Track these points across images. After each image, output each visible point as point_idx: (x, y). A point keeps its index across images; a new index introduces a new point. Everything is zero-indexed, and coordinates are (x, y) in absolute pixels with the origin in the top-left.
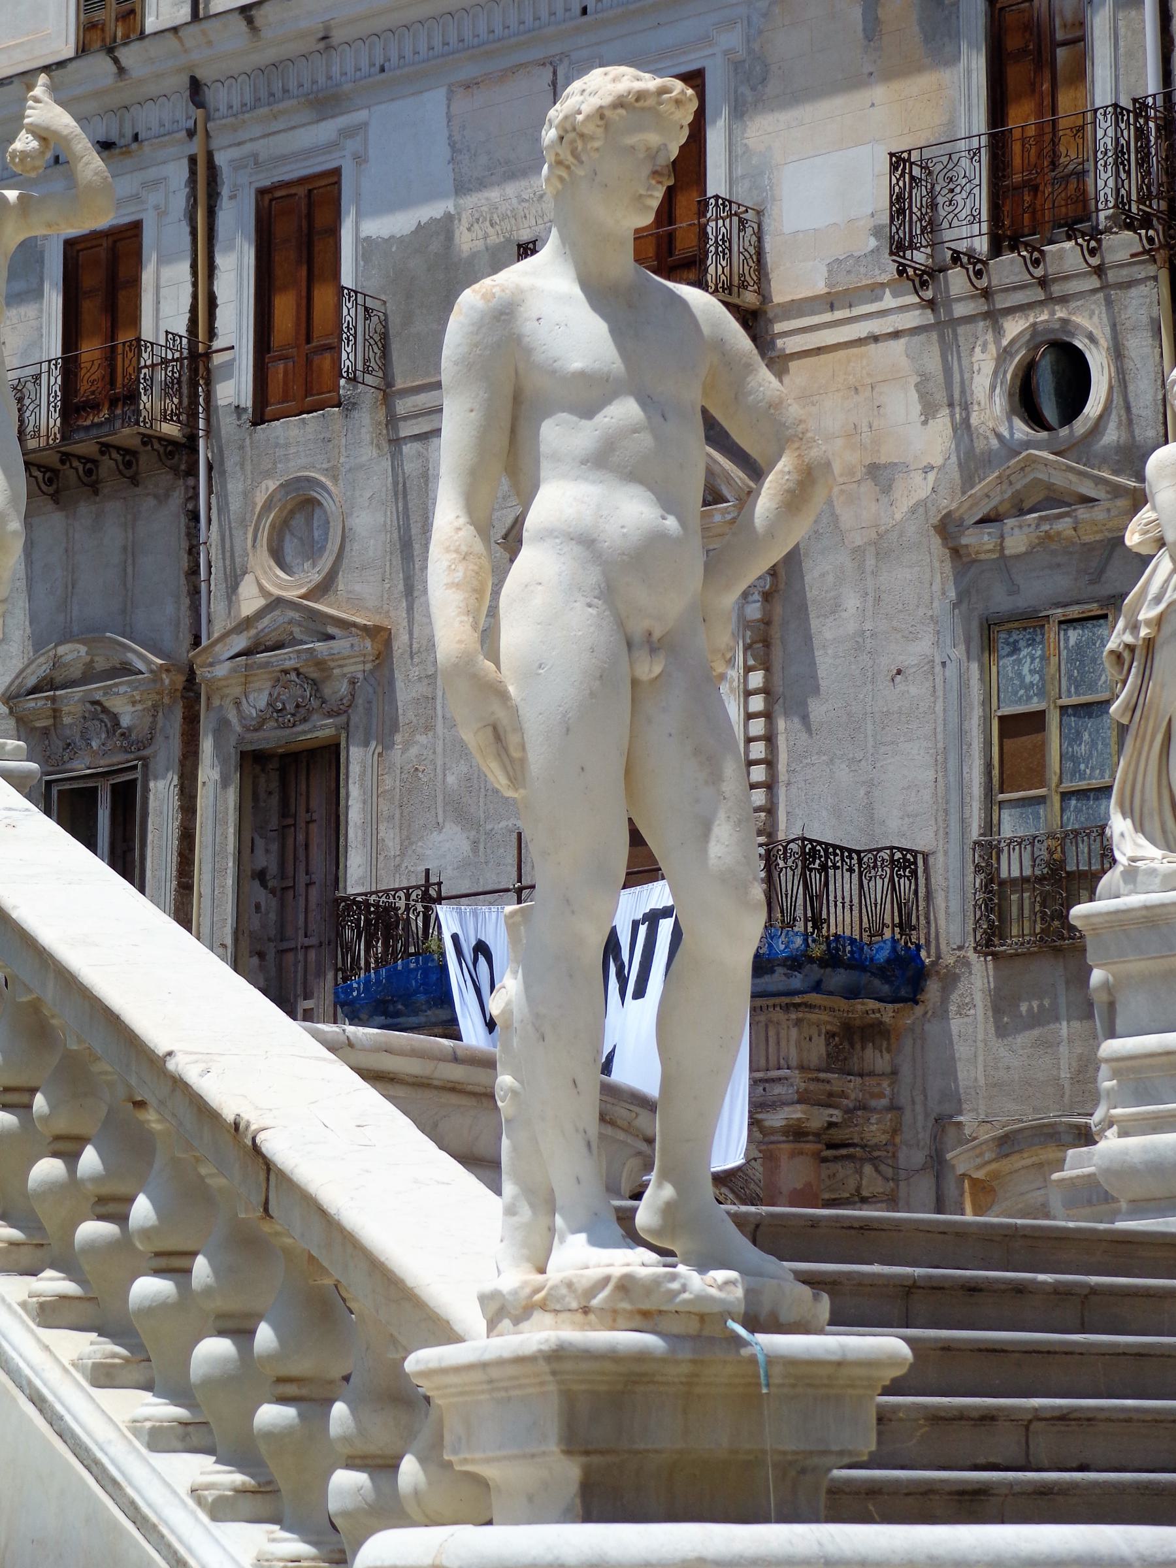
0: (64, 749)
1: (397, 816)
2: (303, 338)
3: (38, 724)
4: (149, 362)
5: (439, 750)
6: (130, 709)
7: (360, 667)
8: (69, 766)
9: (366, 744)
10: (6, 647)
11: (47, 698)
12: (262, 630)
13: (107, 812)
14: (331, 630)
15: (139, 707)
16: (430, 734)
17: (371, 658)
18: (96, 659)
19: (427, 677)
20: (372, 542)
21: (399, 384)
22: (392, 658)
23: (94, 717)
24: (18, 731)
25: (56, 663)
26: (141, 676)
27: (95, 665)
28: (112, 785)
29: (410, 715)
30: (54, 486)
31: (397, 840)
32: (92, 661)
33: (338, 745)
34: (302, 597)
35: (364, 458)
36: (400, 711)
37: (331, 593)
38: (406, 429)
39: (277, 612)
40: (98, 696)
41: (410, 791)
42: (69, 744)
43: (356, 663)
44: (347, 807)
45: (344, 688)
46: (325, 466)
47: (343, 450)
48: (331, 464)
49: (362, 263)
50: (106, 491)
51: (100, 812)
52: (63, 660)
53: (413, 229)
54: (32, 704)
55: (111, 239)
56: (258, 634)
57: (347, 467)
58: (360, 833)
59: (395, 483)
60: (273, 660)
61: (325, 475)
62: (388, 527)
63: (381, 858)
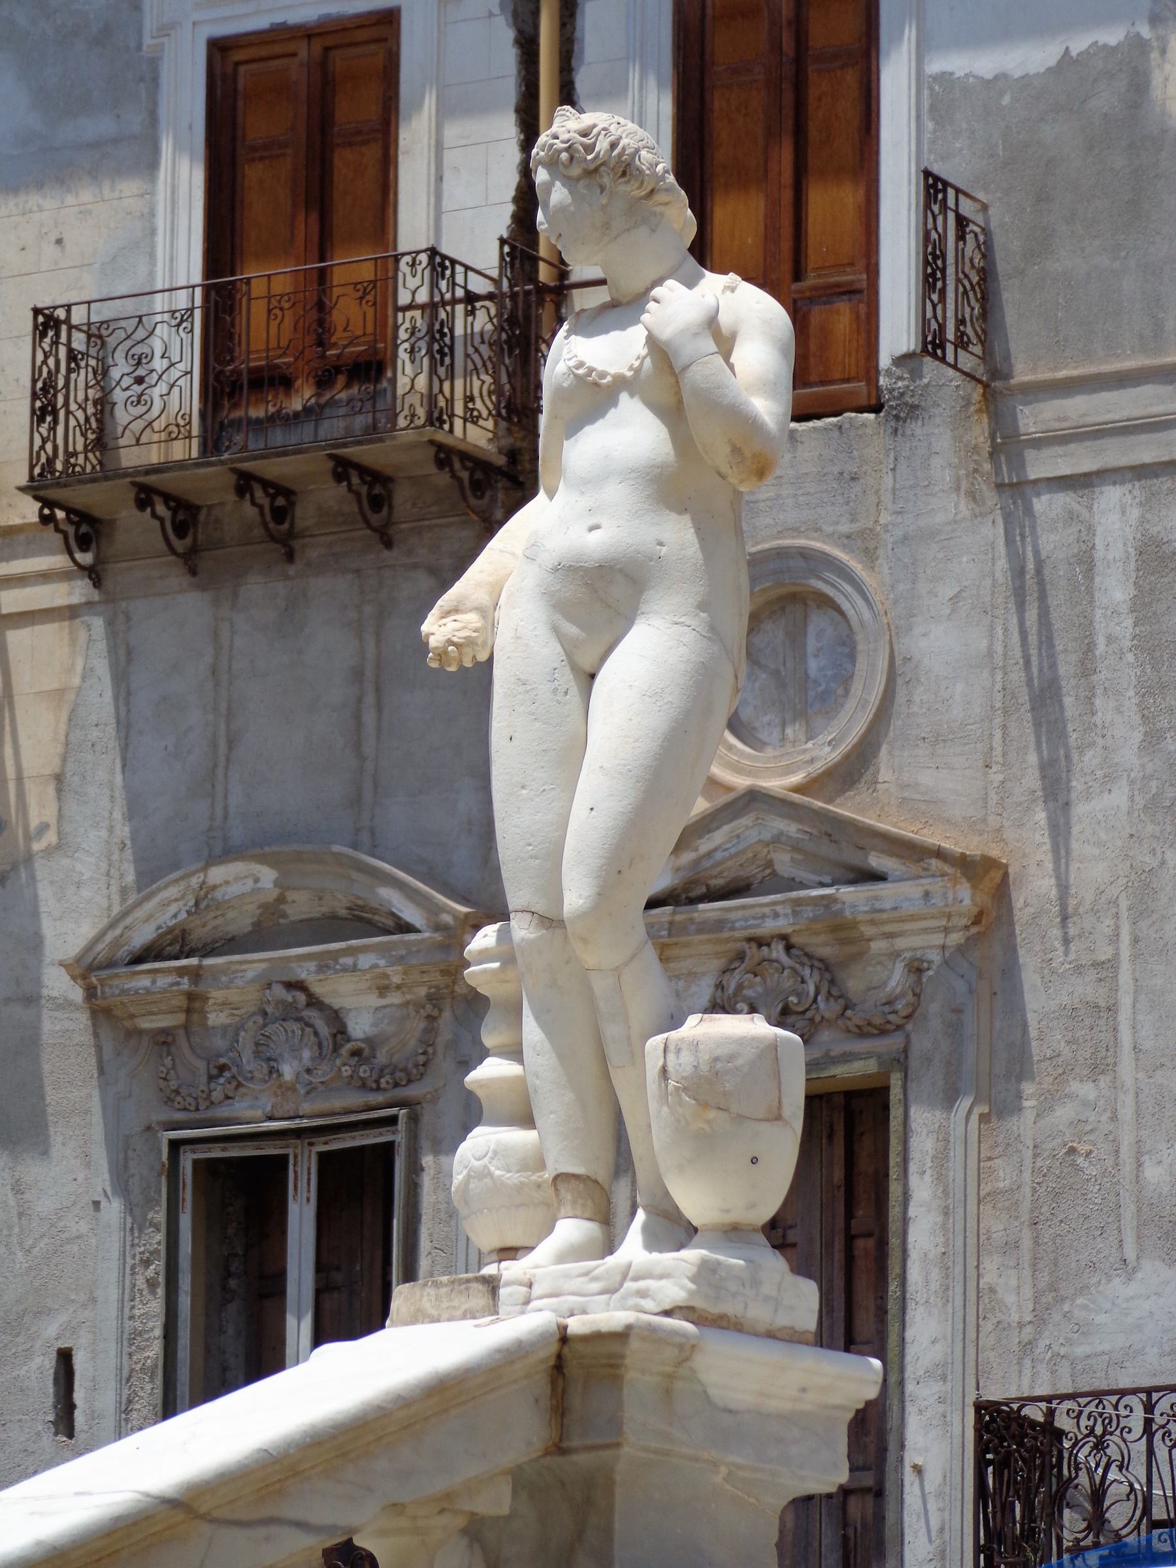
0: (211, 1078)
1: (1027, 1243)
2: (786, 267)
3: (146, 1024)
4: (423, 297)
5: (1127, 1111)
6: (374, 1000)
7: (938, 939)
8: (222, 1112)
9: (950, 1099)
10: (65, 862)
11: (181, 972)
12: (709, 854)
13: (310, 1211)
14: (876, 861)
15: (395, 998)
16: (1104, 1081)
17: (964, 921)
18: (290, 896)
19: (1096, 965)
20: (960, 687)
21: (1022, 374)
22: (1011, 924)
23: (288, 1013)
24: (96, 1035)
25: (203, 901)
26: (412, 937)
27: (288, 909)
28: (323, 1157)
29: (1058, 1039)
30: (188, 541)
31: (1027, 1292)
32: (281, 899)
33: (886, 1089)
34: (798, 789)
35: (940, 518)
36: (1033, 1033)
37: (861, 785)
38: (1040, 466)
39: (746, 821)
40: (305, 973)
41: (1056, 1195)
42: (222, 1068)
43: (926, 931)
44: (905, 1221)
45: (896, 979)
46: (844, 528)
47: (887, 498)
48: (855, 527)
49: (929, 125)
50: (313, 554)
51: (293, 1208)
52: (218, 894)
53: (1052, 62)
54: (145, 982)
55: (317, 46)
56: (697, 862)
57: (899, 533)
58: (935, 1274)
59: (1019, 572)
60: (732, 916)
61: (844, 547)
62: (999, 660)
63: (987, 1326)
